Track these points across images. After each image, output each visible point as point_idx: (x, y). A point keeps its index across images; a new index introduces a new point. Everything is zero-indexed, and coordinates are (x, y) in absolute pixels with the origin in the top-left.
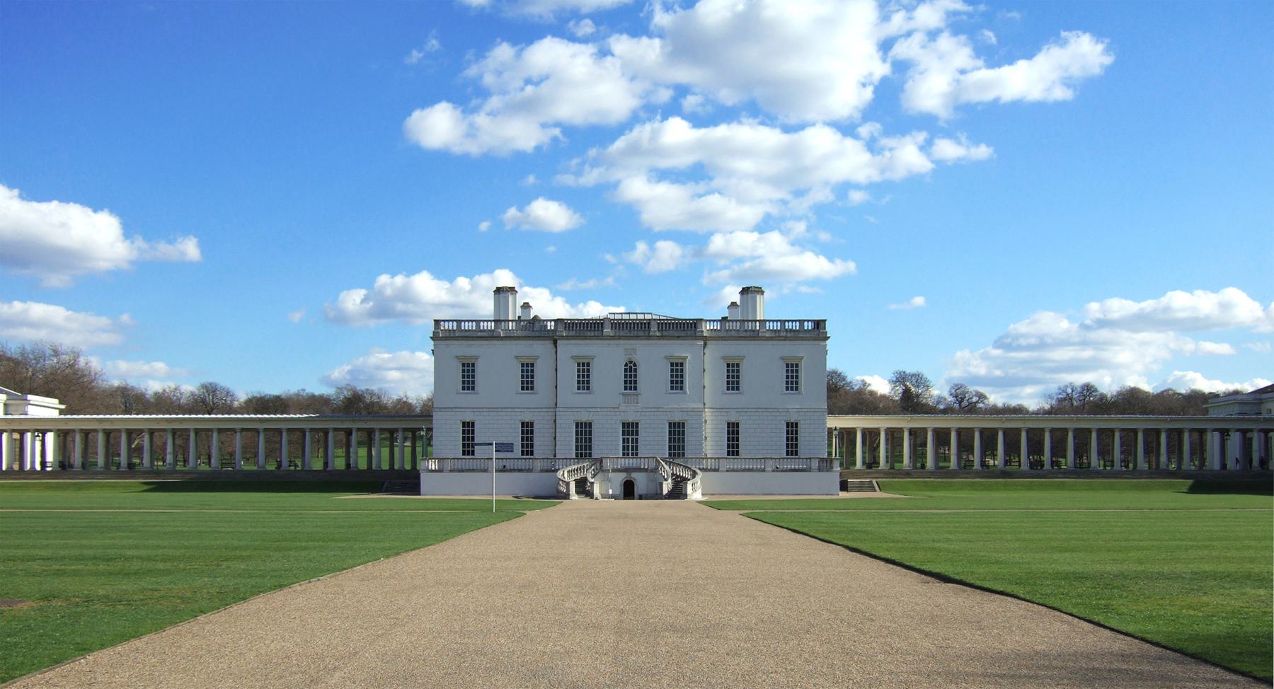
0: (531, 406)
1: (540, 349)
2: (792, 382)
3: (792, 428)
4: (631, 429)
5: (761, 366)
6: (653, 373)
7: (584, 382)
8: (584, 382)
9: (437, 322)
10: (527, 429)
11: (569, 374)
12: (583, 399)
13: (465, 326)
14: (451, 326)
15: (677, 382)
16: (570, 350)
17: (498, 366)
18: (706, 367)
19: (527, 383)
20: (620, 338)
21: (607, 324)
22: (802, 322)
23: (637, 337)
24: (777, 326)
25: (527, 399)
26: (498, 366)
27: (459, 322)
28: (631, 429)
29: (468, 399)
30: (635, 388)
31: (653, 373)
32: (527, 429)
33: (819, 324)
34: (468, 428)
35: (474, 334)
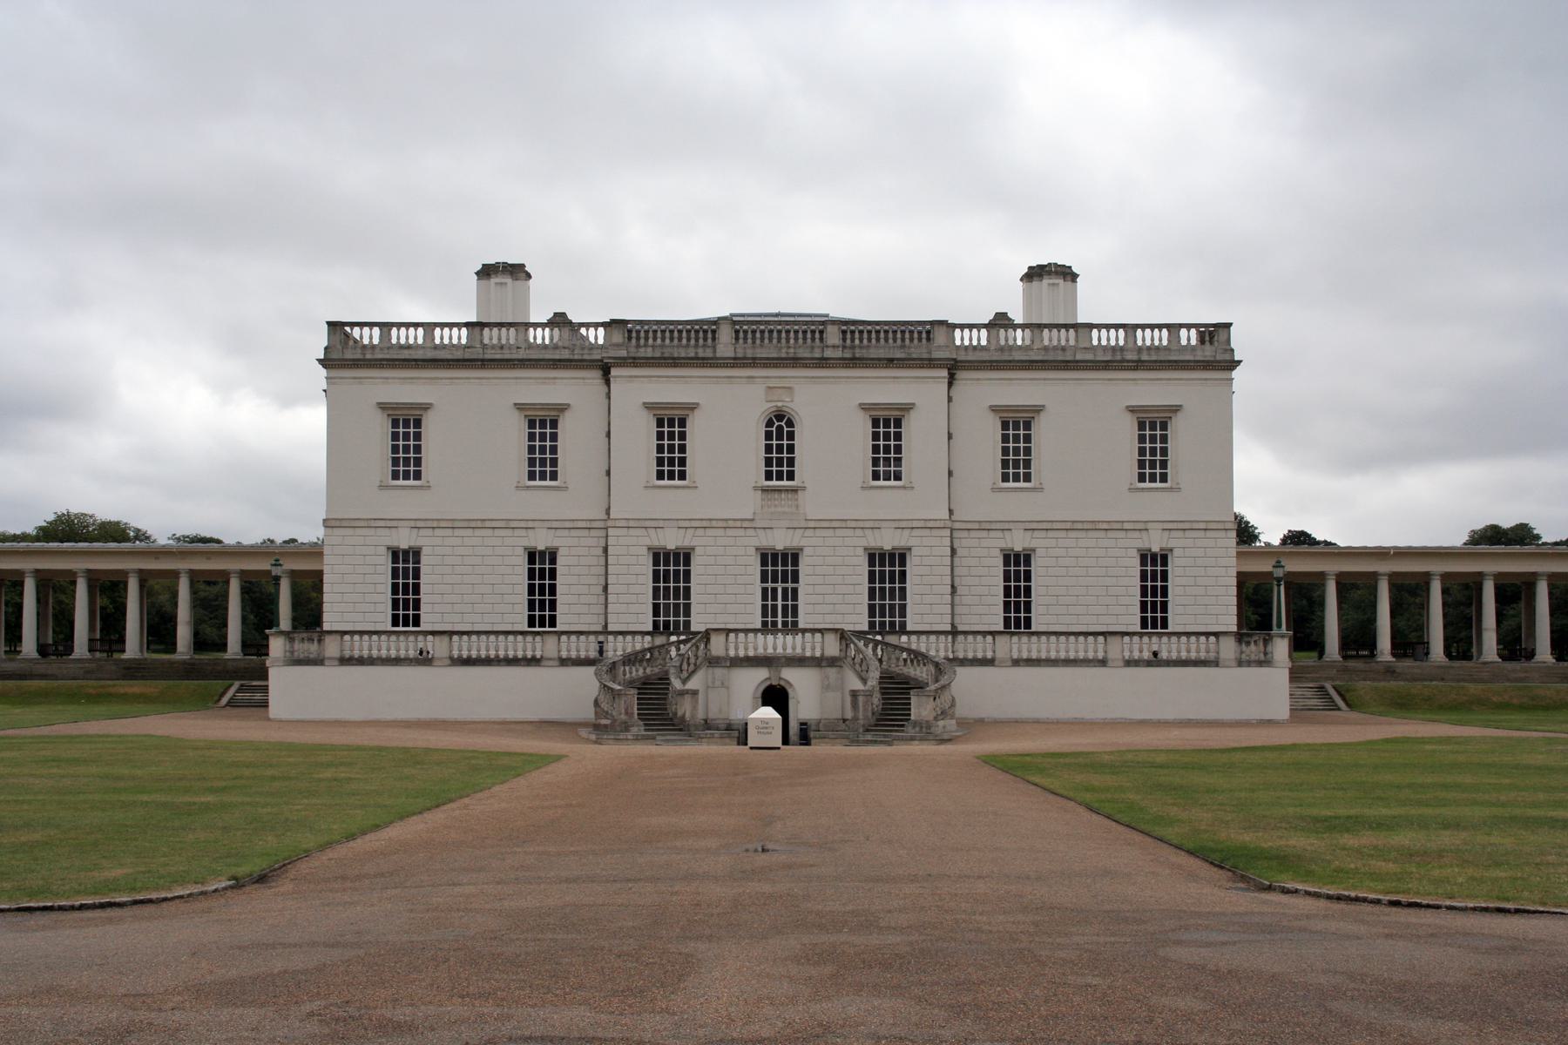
2: (1153, 463)
3: (1155, 567)
4: (780, 567)
5: (1085, 429)
7: (671, 462)
8: (671, 462)
9: (334, 326)
11: (637, 444)
12: (671, 500)
13: (398, 336)
14: (371, 337)
17: (474, 427)
18: (950, 428)
19: (543, 461)
20: (754, 362)
21: (725, 335)
22: (1173, 328)
23: (794, 362)
24: (1118, 338)
25: (542, 502)
26: (474, 427)
27: (385, 327)
28: (780, 567)
29: (406, 502)
30: (791, 476)
32: (542, 567)
33: (1213, 334)
35: (419, 355)
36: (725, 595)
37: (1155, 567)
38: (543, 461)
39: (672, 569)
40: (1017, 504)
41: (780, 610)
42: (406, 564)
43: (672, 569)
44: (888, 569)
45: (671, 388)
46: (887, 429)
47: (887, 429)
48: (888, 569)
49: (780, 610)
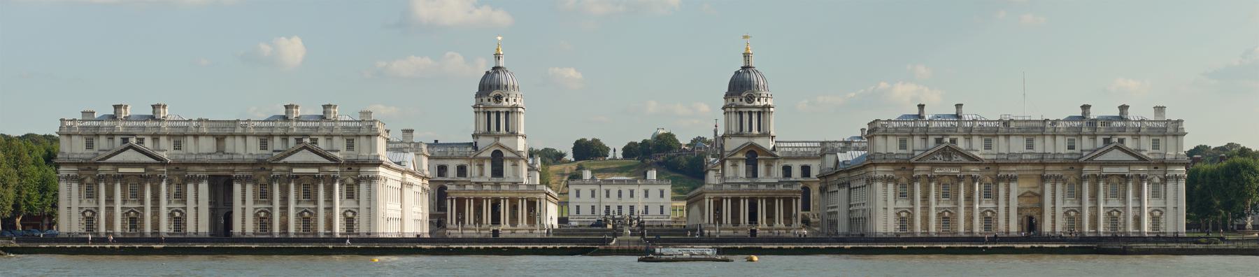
0: (594, 201)
1: (596, 187)
3: (662, 207)
4: (620, 207)
6: (626, 193)
7: (608, 196)
8: (608, 196)
10: (593, 207)
11: (604, 194)
15: (632, 196)
16: (604, 188)
19: (593, 196)
28: (620, 207)
31: (626, 193)
32: (593, 207)
34: (578, 207)
36: (614, 208)
37: (662, 207)
38: (593, 196)
39: (608, 208)
40: (647, 200)
41: (620, 213)
42: (578, 207)
43: (608, 208)
44: (632, 208)
45: (608, 187)
46: (632, 192)
47: (632, 192)
48: (632, 208)
49: (620, 213)
